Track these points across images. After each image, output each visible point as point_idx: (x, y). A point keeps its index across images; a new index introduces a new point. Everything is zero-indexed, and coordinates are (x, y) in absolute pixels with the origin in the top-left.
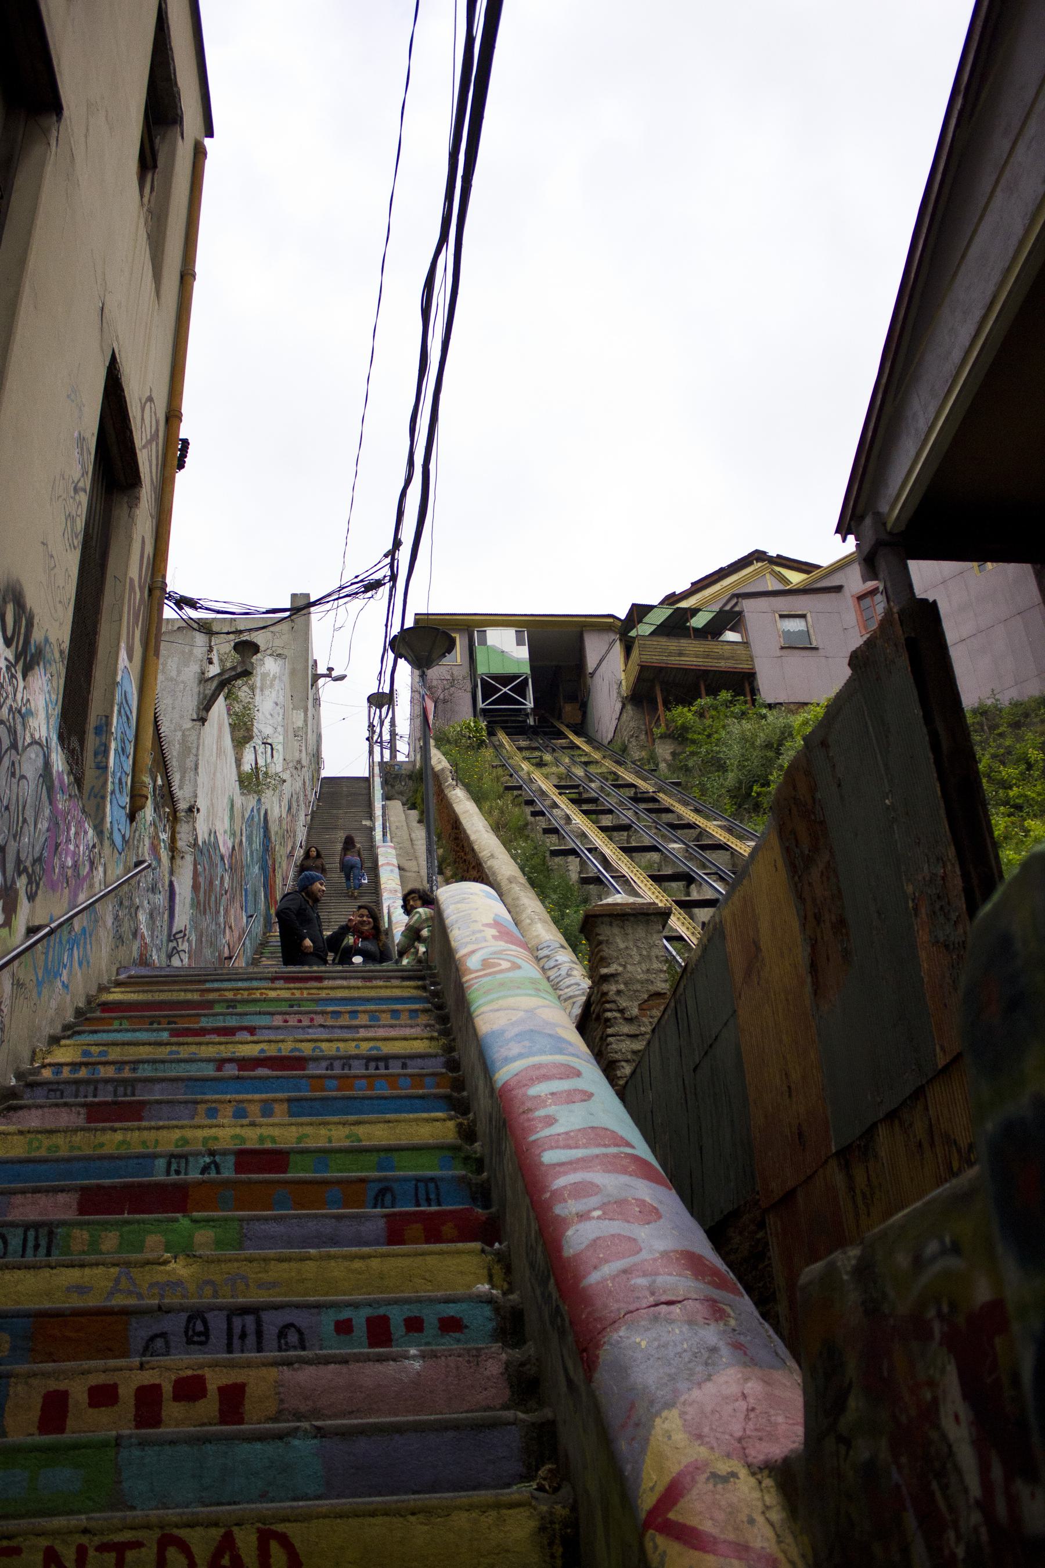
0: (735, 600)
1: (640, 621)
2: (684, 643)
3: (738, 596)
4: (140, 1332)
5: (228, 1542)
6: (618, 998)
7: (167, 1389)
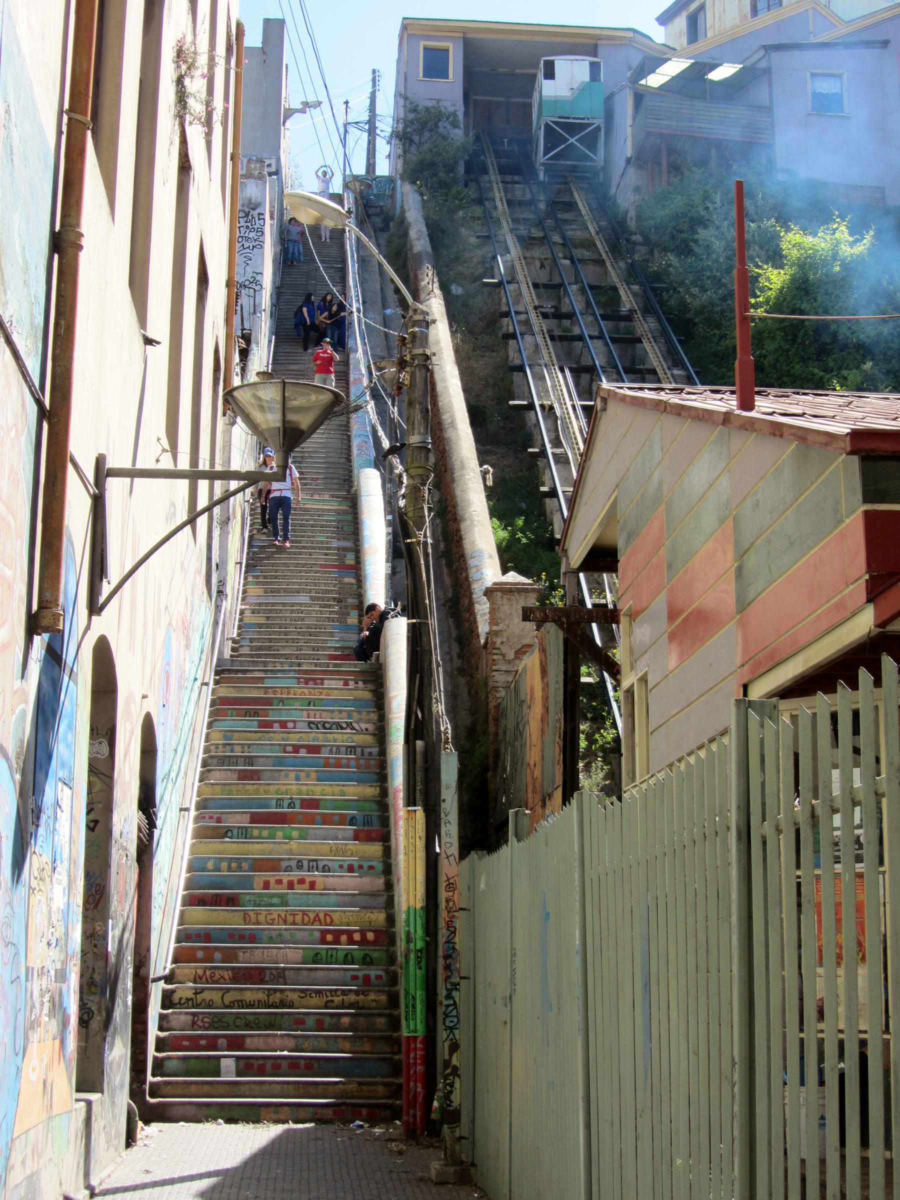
1: (654, 72)
3: (768, 48)
4: (284, 864)
5: (317, 915)
6: (502, 647)
7: (296, 882)
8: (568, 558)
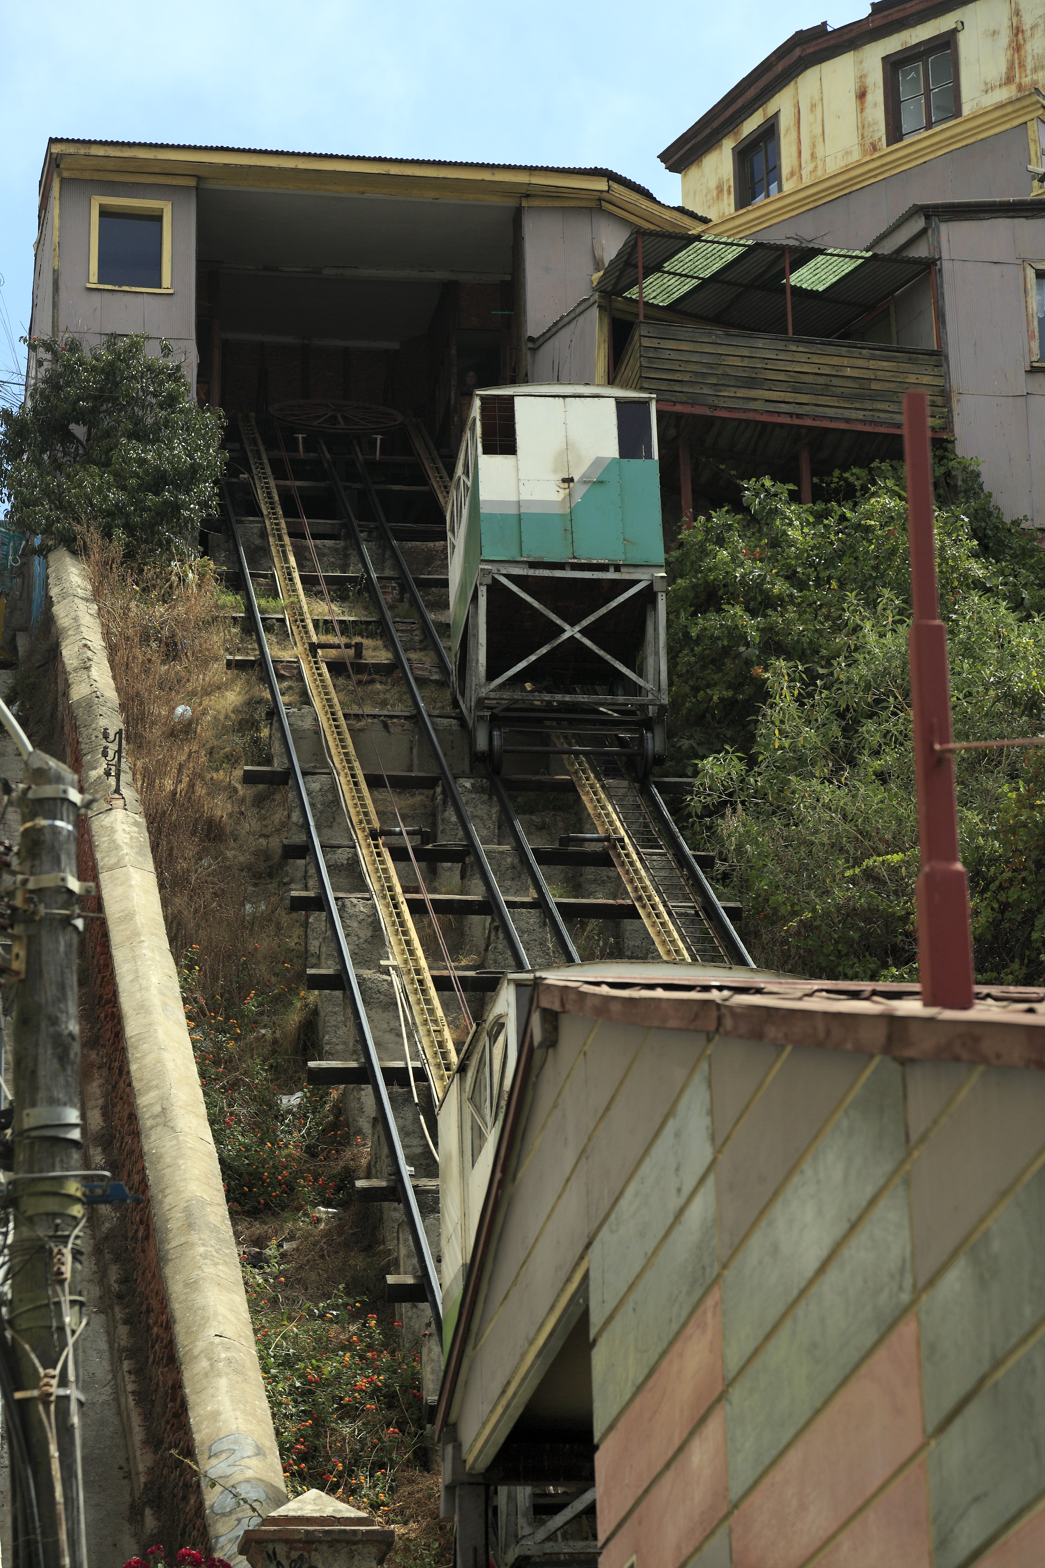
0: (919, 224)
1: (657, 268)
2: (764, 350)
8: (458, 1447)
